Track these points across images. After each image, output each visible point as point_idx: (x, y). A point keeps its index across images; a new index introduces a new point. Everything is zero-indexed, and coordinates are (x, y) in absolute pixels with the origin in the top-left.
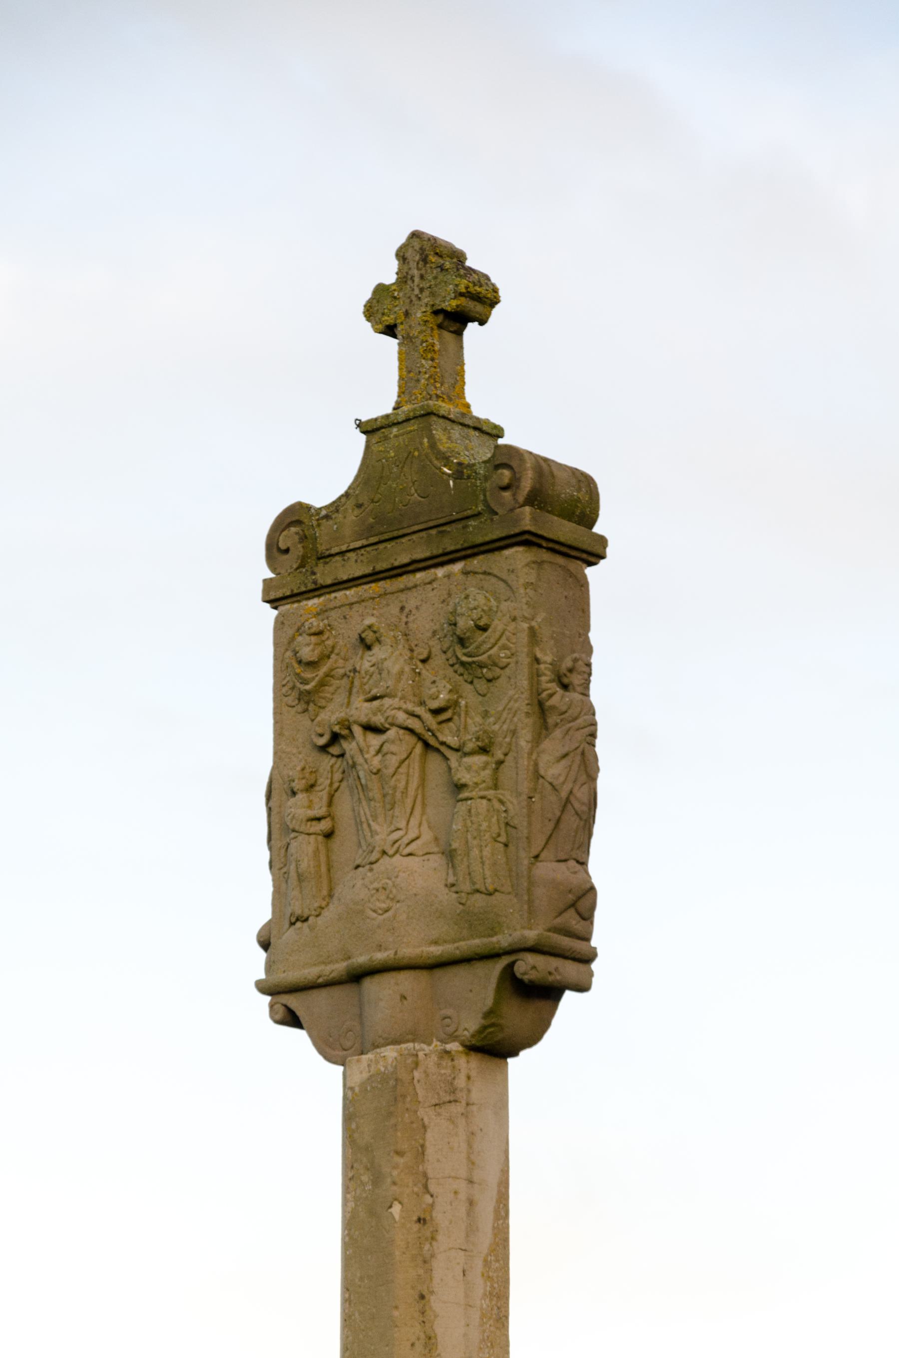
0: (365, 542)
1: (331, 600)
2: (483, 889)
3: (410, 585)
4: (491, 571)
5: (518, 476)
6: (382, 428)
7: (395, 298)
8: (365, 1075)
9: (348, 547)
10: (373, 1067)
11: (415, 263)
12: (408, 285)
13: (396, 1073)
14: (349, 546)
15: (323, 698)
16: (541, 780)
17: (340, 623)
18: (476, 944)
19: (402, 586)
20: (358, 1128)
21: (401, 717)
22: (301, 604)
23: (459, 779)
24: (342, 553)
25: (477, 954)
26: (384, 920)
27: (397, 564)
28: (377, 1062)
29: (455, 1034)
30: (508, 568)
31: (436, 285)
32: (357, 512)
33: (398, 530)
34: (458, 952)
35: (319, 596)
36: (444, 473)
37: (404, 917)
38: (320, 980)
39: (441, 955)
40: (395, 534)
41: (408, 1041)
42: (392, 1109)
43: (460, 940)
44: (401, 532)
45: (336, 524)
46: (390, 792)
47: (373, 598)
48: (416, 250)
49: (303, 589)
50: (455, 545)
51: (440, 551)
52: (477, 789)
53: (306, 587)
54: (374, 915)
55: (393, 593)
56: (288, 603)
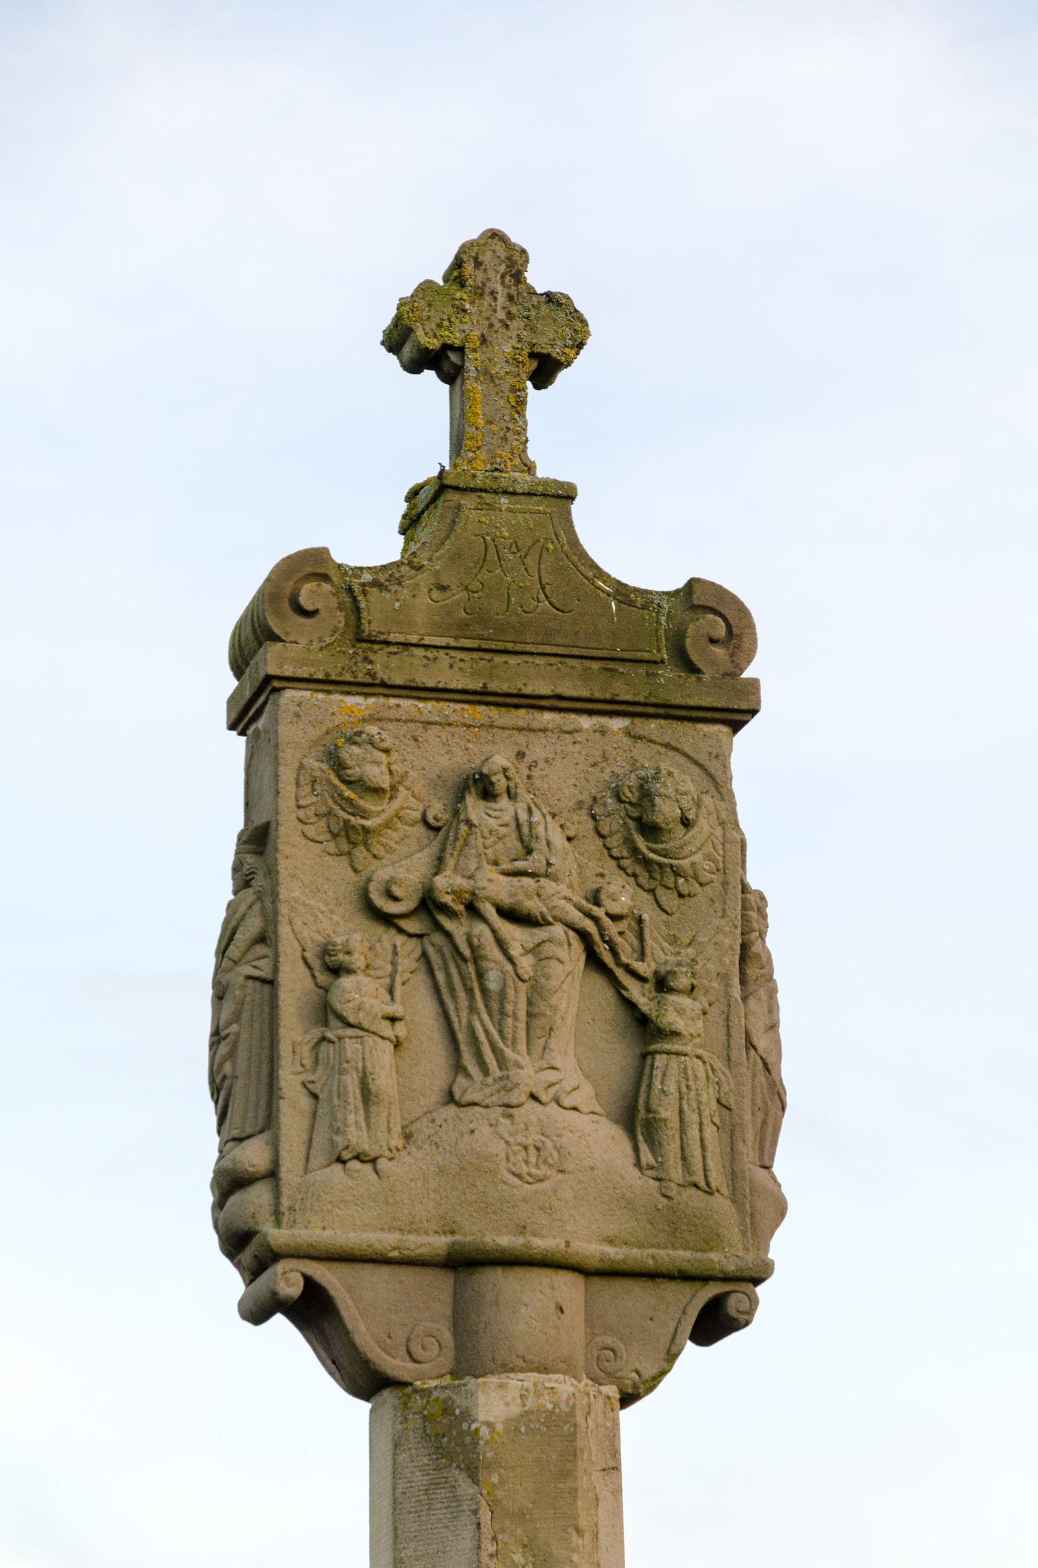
0: (453, 643)
1: (390, 707)
2: (702, 1184)
3: (536, 725)
4: (679, 746)
5: (735, 631)
6: (481, 490)
7: (465, 311)
8: (516, 1410)
9: (420, 640)
10: (530, 1399)
11: (499, 276)
12: (484, 299)
13: (574, 1416)
14: (423, 639)
15: (383, 845)
16: (752, 1052)
17: (406, 745)
18: (682, 1257)
19: (521, 723)
20: (502, 1483)
21: (575, 916)
22: (332, 697)
23: (670, 1024)
24: (406, 645)
25: (680, 1271)
26: (536, 1192)
27: (527, 691)
28: (538, 1395)
29: (618, 1374)
30: (710, 749)
31: (537, 318)
32: (436, 594)
33: (515, 642)
34: (651, 1262)
35: (367, 695)
36: (599, 588)
37: (568, 1195)
38: (395, 1254)
39: (624, 1261)
40: (510, 646)
41: (558, 1372)
42: (569, 1466)
43: (652, 1246)
44: (518, 647)
45: (398, 600)
46: (549, 1013)
47: (469, 726)
48: (499, 257)
49: (348, 677)
50: (634, 695)
51: (608, 696)
52: (691, 1044)
53: (355, 677)
54: (516, 1181)
55: (503, 728)
56: (311, 690)
